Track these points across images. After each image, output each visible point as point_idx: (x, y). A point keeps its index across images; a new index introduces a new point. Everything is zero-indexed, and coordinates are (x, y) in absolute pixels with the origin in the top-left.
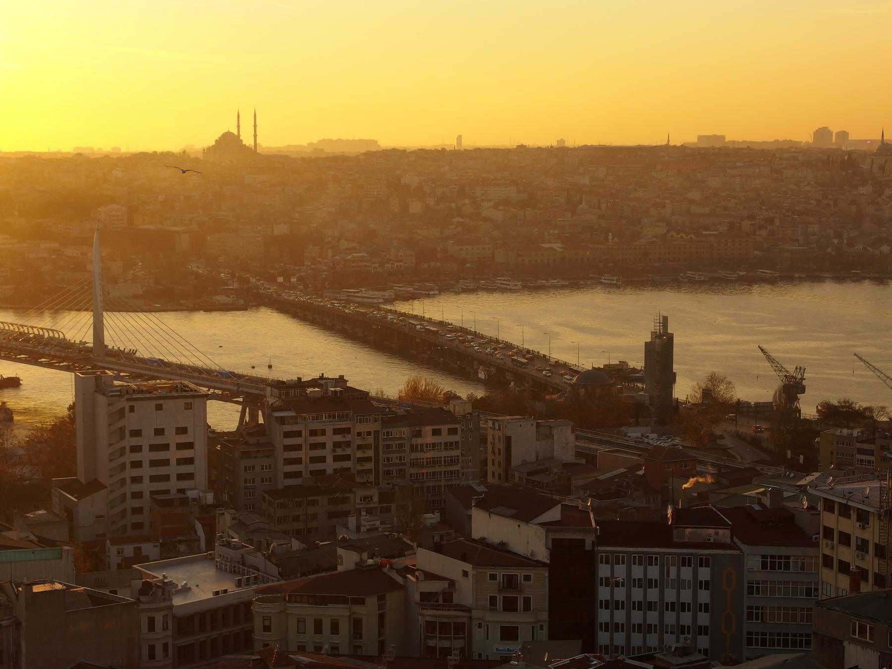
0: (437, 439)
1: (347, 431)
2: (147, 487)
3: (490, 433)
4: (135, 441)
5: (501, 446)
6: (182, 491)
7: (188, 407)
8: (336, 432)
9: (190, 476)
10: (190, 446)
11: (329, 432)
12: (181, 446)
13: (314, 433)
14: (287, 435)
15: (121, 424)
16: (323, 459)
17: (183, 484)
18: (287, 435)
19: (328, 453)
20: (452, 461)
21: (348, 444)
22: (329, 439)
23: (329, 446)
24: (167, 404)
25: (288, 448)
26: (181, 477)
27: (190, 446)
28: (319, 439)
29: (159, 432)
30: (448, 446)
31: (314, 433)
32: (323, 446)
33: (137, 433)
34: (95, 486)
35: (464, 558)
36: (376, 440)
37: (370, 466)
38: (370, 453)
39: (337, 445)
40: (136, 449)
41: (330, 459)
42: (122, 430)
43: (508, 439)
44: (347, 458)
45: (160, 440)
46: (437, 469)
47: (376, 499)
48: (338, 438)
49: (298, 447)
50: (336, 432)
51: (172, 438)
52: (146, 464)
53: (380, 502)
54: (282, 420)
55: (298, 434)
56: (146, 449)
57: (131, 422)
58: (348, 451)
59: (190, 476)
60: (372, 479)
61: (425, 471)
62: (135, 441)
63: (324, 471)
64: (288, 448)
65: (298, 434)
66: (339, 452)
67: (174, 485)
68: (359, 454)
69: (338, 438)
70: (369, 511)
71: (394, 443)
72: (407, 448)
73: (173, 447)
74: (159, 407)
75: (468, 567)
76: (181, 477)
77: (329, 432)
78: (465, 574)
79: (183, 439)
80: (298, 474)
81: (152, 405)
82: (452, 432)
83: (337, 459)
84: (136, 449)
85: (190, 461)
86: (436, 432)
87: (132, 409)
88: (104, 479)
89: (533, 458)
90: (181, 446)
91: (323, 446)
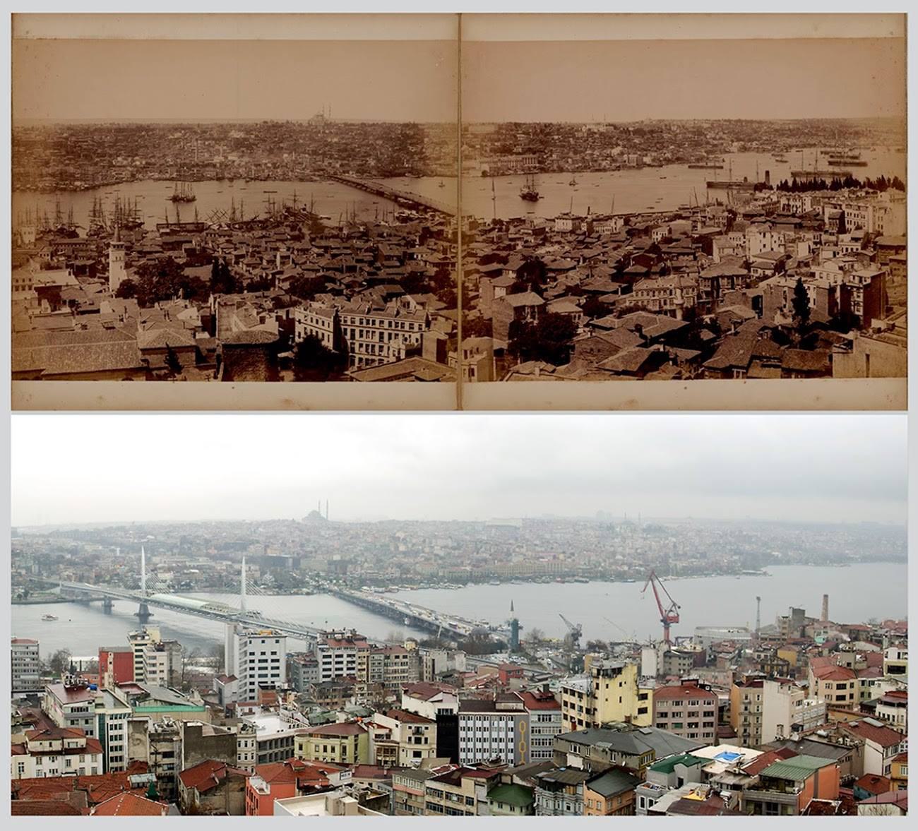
0: (397, 660)
1: (354, 655)
2: (256, 680)
3: (425, 658)
4: (252, 658)
5: (430, 664)
6: (273, 682)
7: (277, 642)
8: (349, 656)
9: (278, 675)
10: (278, 661)
11: (345, 656)
12: (273, 661)
13: (337, 656)
14: (324, 657)
15: (245, 649)
16: (342, 669)
17: (273, 679)
18: (325, 657)
19: (344, 666)
20: (403, 671)
21: (354, 662)
22: (345, 659)
23: (345, 663)
24: (266, 640)
25: (324, 663)
26: (273, 676)
27: (278, 661)
28: (340, 659)
29: (263, 653)
30: (402, 664)
31: (337, 656)
32: (342, 663)
33: (252, 654)
34: (232, 678)
35: (396, 718)
36: (368, 660)
37: (365, 673)
38: (365, 667)
39: (348, 662)
40: (252, 661)
41: (345, 669)
42: (245, 652)
43: (433, 660)
44: (353, 669)
45: (264, 657)
46: (397, 675)
47: (366, 689)
48: (349, 659)
49: (330, 663)
50: (349, 656)
51: (269, 657)
52: (256, 669)
53: (368, 690)
54: (322, 650)
55: (330, 656)
56: (257, 661)
57: (250, 648)
58: (354, 665)
59: (278, 675)
60: (365, 679)
61: (391, 676)
62: (252, 658)
63: (342, 675)
64: (324, 663)
65: (330, 656)
66: (350, 666)
67: (269, 680)
68: (359, 667)
69: (349, 659)
70: (362, 695)
71: (376, 662)
72: (383, 664)
73: (269, 661)
74: (263, 642)
75: (398, 723)
76: (273, 676)
77: (345, 656)
78: (397, 726)
79: (274, 657)
80: (329, 676)
81: (260, 640)
82: (405, 657)
83: (348, 669)
84: (252, 661)
85: (278, 668)
86: (397, 657)
87: (250, 642)
88: (237, 675)
89: (446, 670)
90: (273, 661)
91: (342, 663)
